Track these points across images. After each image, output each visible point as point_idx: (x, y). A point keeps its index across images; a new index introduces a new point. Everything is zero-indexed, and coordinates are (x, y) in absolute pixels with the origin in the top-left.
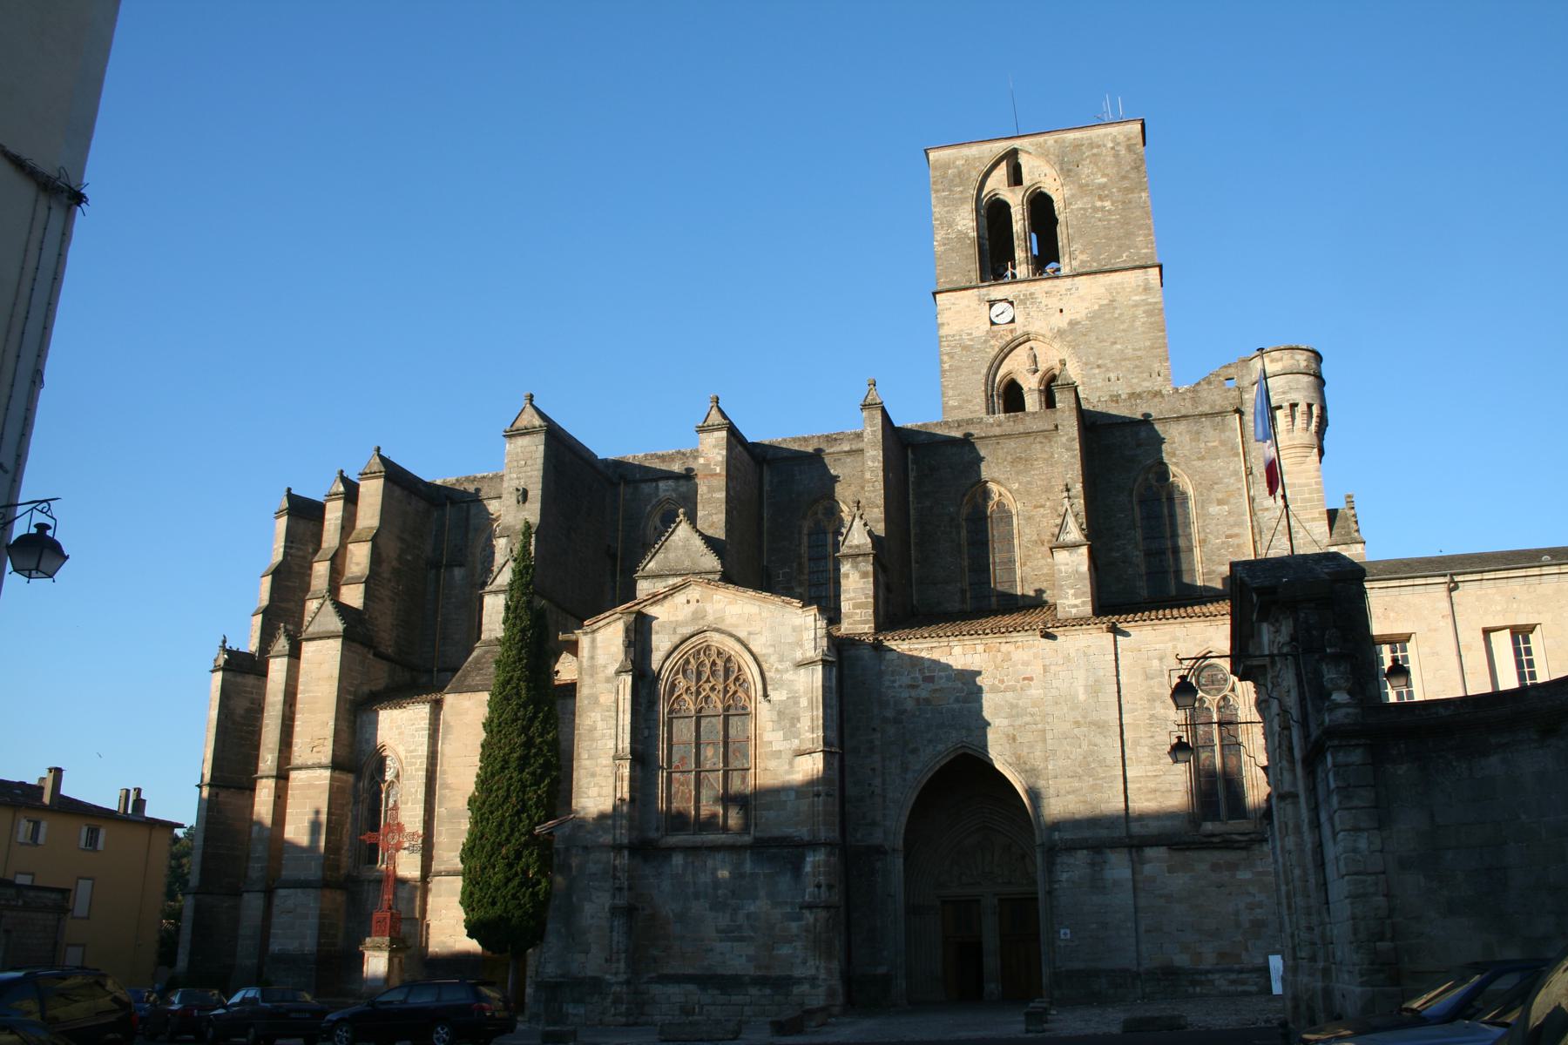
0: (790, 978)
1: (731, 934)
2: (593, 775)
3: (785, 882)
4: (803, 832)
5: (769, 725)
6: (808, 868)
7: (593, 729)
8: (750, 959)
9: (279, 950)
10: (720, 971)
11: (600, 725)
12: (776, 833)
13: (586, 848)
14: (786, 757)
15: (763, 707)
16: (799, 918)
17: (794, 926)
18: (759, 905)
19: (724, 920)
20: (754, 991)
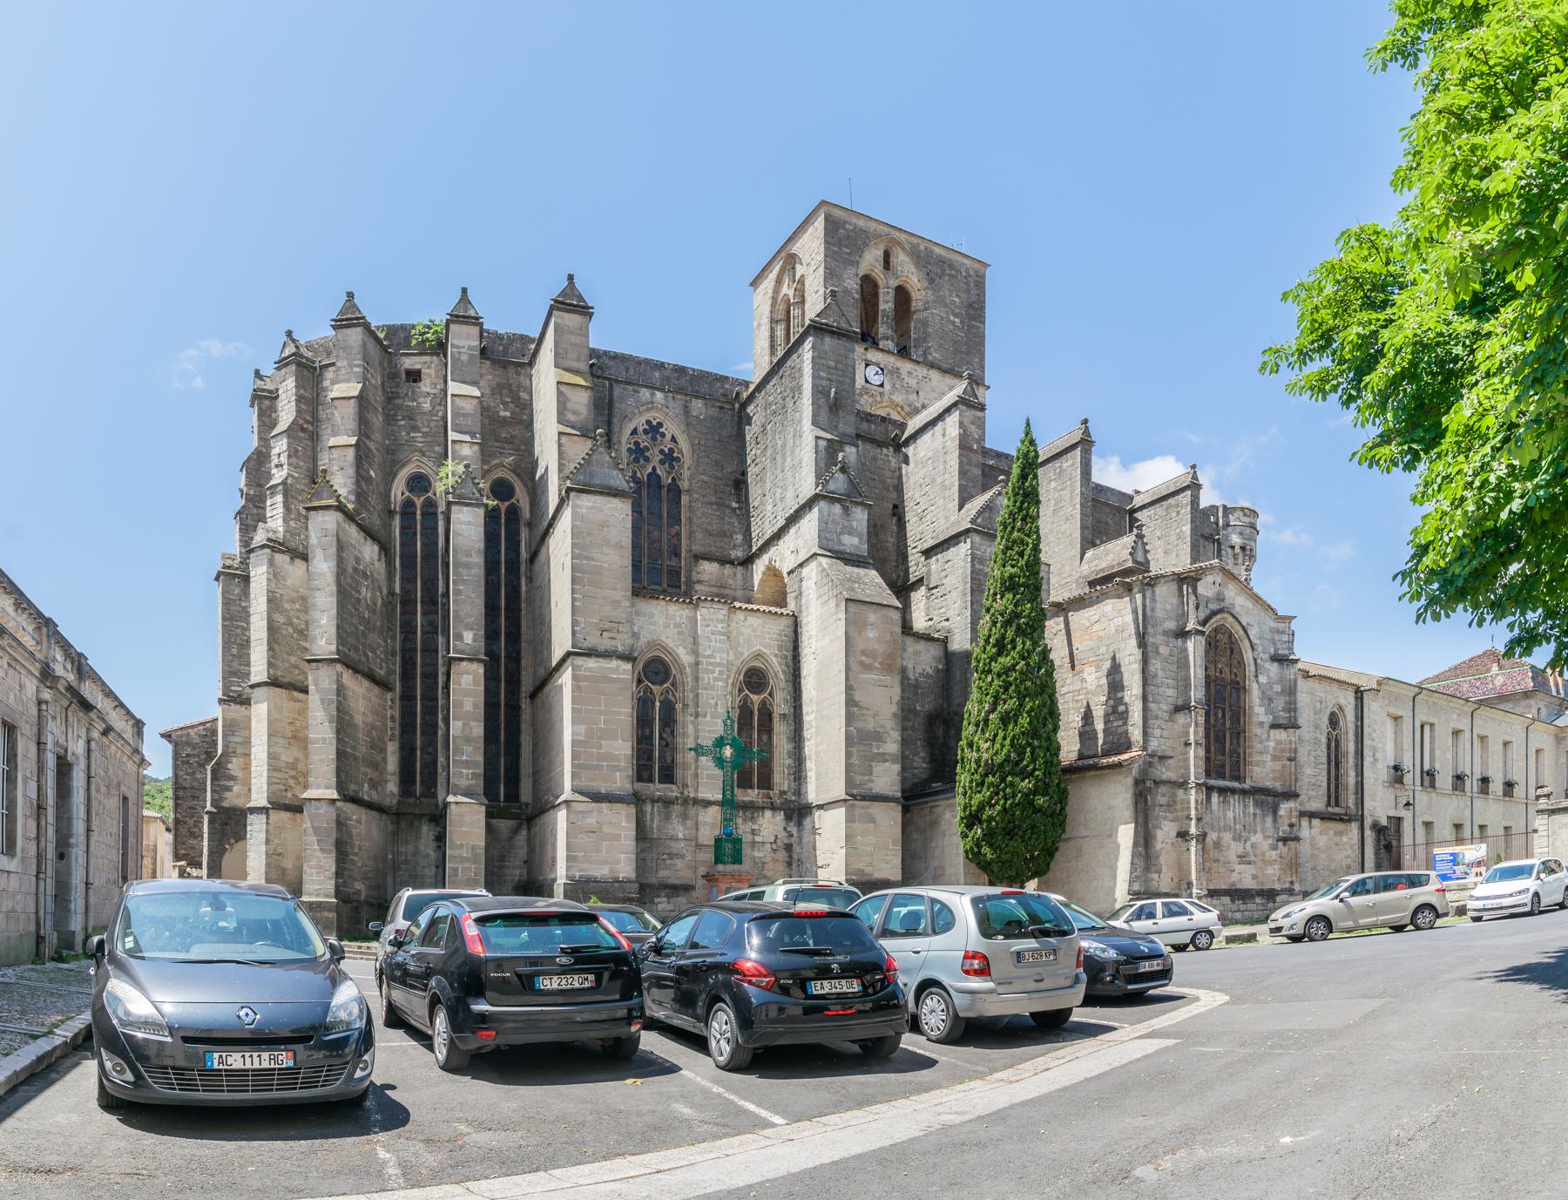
0: (1274, 890)
1: (1243, 859)
2: (1157, 718)
3: (1269, 819)
4: (1278, 786)
5: (1257, 701)
6: (1282, 812)
7: (1156, 676)
8: (1254, 877)
9: (581, 877)
10: (1239, 887)
11: (1160, 673)
12: (1261, 785)
13: (1155, 781)
14: (1266, 726)
15: (1255, 686)
16: (1275, 848)
17: (1274, 853)
18: (1257, 838)
19: (1240, 850)
20: (1258, 900)
